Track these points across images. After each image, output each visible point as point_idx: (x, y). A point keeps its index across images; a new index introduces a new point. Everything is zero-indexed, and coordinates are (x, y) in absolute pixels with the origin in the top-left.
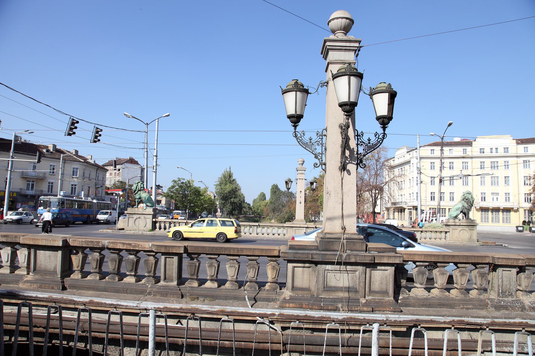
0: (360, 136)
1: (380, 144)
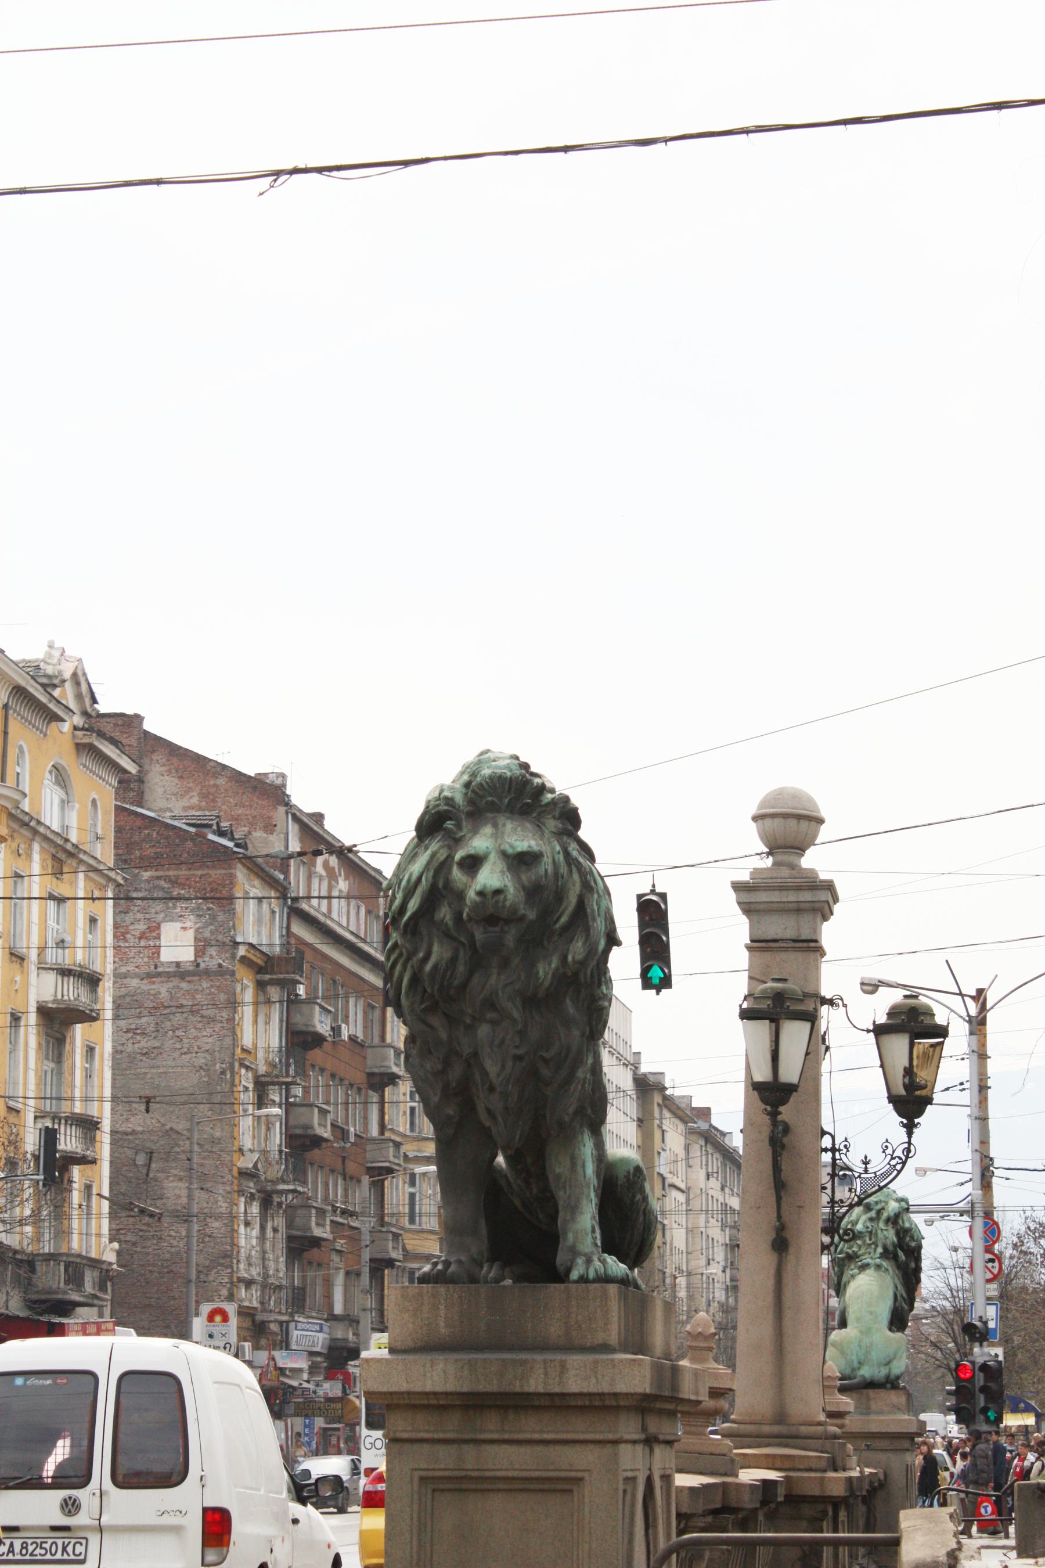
0: (839, 1150)
1: (895, 1172)
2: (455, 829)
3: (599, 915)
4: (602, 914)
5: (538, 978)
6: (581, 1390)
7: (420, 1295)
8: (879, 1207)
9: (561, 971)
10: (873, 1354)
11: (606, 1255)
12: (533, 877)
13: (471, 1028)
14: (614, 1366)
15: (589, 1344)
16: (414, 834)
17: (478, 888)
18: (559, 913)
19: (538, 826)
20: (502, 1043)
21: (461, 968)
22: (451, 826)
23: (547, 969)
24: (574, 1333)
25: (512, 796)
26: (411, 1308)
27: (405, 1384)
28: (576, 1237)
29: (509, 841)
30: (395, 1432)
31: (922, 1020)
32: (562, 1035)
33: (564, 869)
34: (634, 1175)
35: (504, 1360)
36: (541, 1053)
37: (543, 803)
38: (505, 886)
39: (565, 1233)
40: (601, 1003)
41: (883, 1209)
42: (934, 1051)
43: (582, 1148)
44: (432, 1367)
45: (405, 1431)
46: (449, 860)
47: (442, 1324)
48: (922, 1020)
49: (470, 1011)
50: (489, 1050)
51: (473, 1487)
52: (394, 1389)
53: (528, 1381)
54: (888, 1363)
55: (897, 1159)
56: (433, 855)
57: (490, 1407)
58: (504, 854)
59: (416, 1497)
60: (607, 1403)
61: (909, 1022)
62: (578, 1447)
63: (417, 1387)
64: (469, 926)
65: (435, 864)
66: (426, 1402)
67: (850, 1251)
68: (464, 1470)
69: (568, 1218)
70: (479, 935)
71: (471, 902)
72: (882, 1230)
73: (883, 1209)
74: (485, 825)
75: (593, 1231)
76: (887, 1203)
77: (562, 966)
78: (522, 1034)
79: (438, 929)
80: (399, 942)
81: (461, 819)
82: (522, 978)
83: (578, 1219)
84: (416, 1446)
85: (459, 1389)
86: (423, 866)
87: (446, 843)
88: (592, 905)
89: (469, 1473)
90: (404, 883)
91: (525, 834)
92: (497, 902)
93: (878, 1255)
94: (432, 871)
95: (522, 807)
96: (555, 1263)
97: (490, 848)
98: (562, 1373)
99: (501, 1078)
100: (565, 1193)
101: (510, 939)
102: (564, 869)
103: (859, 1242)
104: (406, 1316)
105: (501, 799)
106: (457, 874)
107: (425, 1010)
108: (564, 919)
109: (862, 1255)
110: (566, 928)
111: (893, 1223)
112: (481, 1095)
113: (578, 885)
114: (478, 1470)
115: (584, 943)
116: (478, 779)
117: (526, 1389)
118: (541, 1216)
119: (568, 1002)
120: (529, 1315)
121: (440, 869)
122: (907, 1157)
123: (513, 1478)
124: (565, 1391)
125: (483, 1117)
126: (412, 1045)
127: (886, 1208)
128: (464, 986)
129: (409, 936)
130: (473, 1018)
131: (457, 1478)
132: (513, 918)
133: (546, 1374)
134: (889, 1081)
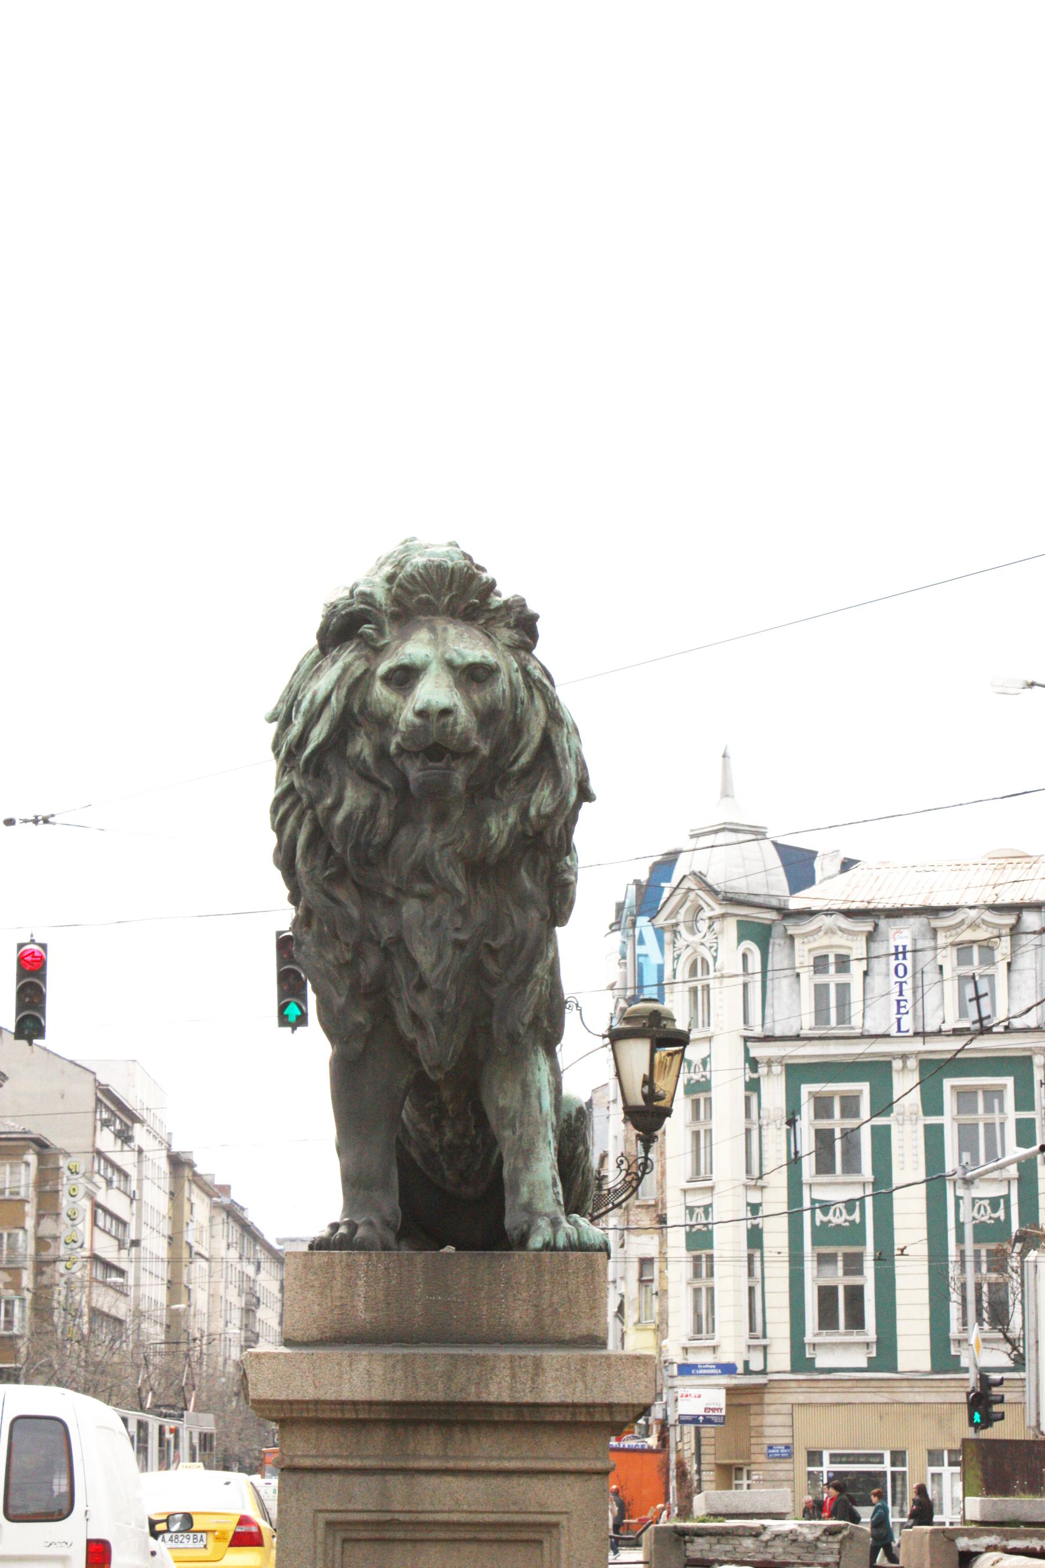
2: (375, 636)
3: (571, 756)
4: (574, 756)
5: (489, 838)
6: (563, 1399)
7: (331, 1264)
9: (520, 828)
11: (576, 1216)
12: (488, 698)
13: (392, 905)
14: (609, 1367)
15: (567, 1337)
16: (315, 642)
17: (419, 706)
18: (517, 751)
19: (489, 637)
20: (437, 924)
21: (384, 821)
22: (370, 631)
23: (501, 824)
24: (547, 1321)
25: (454, 593)
26: (317, 1284)
27: (311, 1390)
28: (532, 1191)
29: (457, 648)
30: (292, 1458)
31: (665, 1025)
32: (515, 919)
33: (523, 693)
34: (577, 1119)
35: (452, 1356)
36: (486, 941)
37: (492, 607)
38: (455, 705)
39: (516, 1189)
40: (566, 876)
42: (672, 1060)
43: (537, 1071)
44: (351, 1365)
45: (306, 1456)
46: (367, 676)
47: (361, 1306)
48: (665, 1025)
49: (393, 880)
50: (420, 934)
51: (400, 1535)
52: (297, 1396)
53: (487, 1386)
55: (633, 1175)
56: (345, 670)
57: (428, 1423)
58: (450, 665)
59: (320, 1549)
60: (597, 1418)
61: (651, 1026)
62: (551, 1480)
63: (330, 1395)
64: (398, 763)
65: (348, 680)
66: (340, 1415)
68: (389, 1511)
69: (520, 1164)
70: (414, 772)
71: (407, 726)
74: (418, 629)
75: (555, 1185)
77: (522, 823)
78: (464, 912)
79: (351, 768)
80: (297, 785)
81: (384, 622)
82: (467, 835)
83: (534, 1168)
84: (323, 1478)
85: (389, 1398)
86: (333, 683)
87: (364, 653)
88: (562, 741)
89: (396, 1516)
90: (305, 705)
91: (474, 642)
92: (444, 726)
94: (345, 689)
95: (466, 608)
96: (504, 1226)
97: (431, 656)
98: (537, 1375)
99: (436, 973)
100: (514, 1133)
101: (459, 778)
102: (523, 693)
104: (310, 1295)
105: (438, 597)
106: (380, 691)
107: (330, 879)
108: (524, 759)
110: (527, 772)
112: (405, 995)
113: (542, 714)
114: (410, 1512)
115: (553, 791)
116: (408, 568)
117: (485, 1398)
118: (447, 1173)
119: (524, 874)
120: (483, 1294)
121: (359, 685)
122: (644, 1173)
123: (459, 1524)
124: (538, 1401)
125: (404, 1024)
126: (304, 929)
128: (386, 846)
129: (311, 778)
130: (397, 890)
131: (378, 1523)
132: (464, 753)
133: (513, 1376)
134: (626, 1091)
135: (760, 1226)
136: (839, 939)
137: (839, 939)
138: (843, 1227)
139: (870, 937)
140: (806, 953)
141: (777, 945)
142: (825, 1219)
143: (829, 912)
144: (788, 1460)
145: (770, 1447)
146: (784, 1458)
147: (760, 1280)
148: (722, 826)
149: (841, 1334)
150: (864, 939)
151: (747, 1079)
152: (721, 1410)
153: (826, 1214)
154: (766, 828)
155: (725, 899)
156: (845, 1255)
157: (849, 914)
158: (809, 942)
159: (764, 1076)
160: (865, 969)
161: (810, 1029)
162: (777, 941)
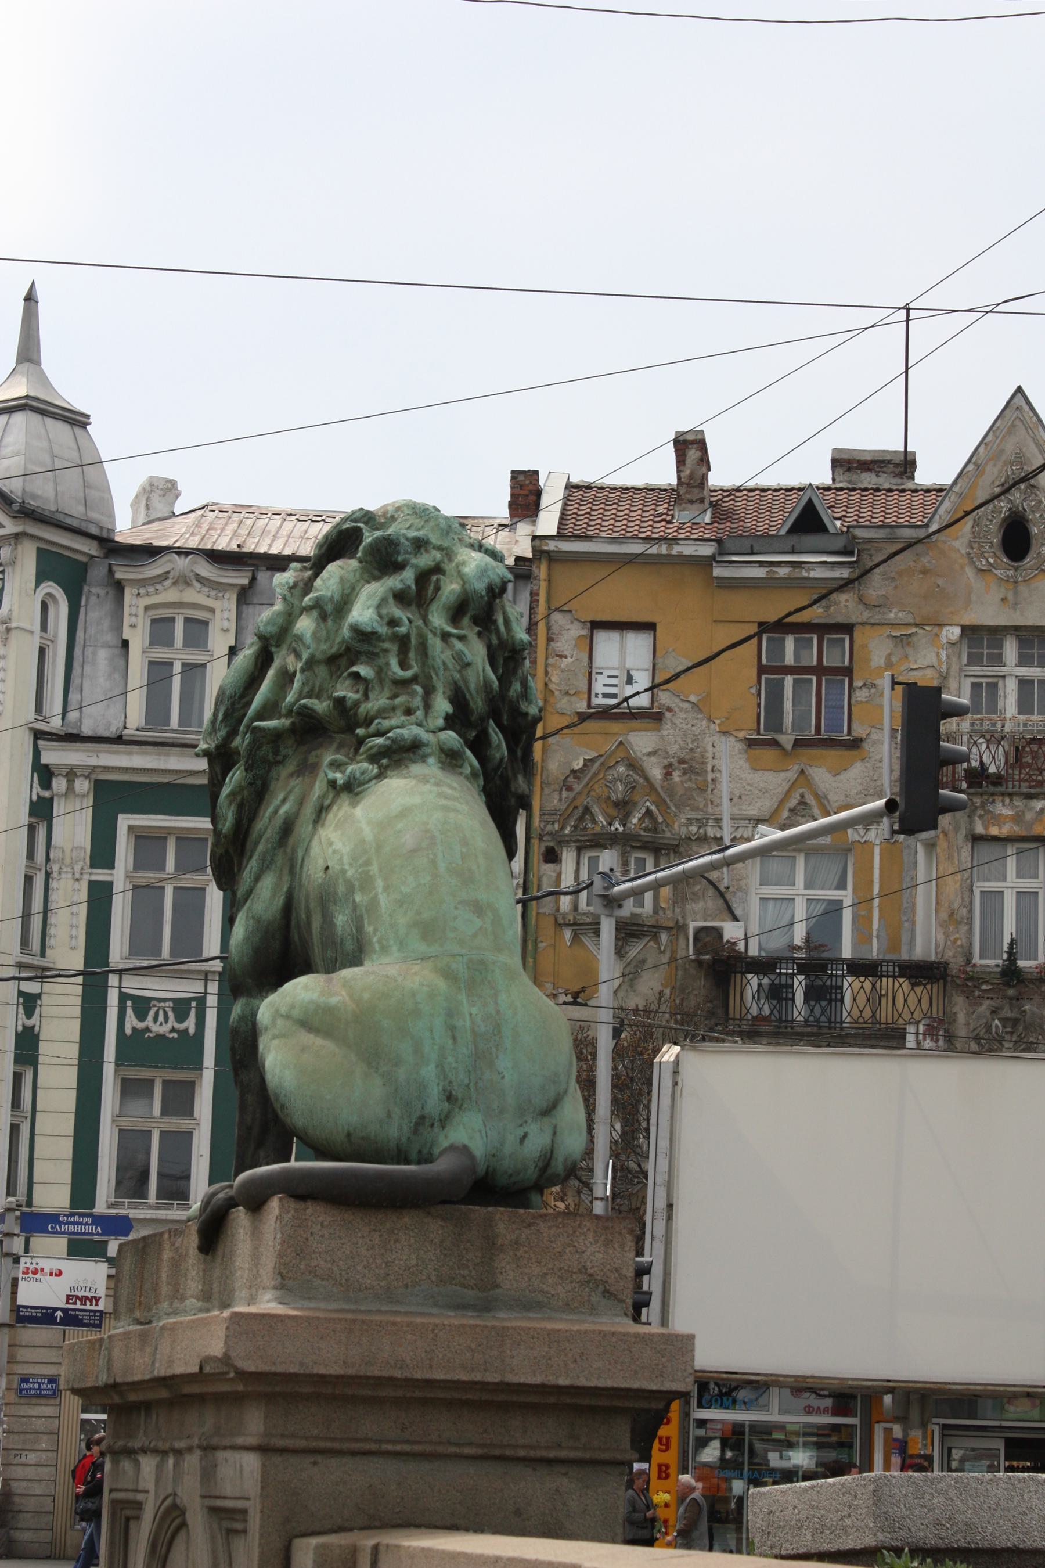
8: (425, 560)
10: (504, 1063)
41: (438, 569)
54: (549, 1110)
67: (321, 706)
72: (445, 636)
73: (438, 569)
76: (448, 553)
93: (440, 722)
103: (363, 670)
109: (382, 713)
111: (476, 621)
127: (450, 567)
135: (37, 1029)
136: (194, 595)
137: (194, 595)
138: (168, 1038)
139: (244, 596)
140: (141, 611)
141: (95, 593)
142: (140, 1025)
143: (183, 552)
144: (52, 1401)
145: (25, 1380)
146: (47, 1397)
147: (29, 1115)
148: (23, 402)
149: (150, 1207)
150: (235, 597)
151: (35, 798)
152: (98, 1300)
153: (141, 1016)
154: (88, 417)
155: (19, 512)
156: (166, 1083)
157: (217, 557)
158: (148, 595)
159: (60, 796)
160: (233, 644)
161: (138, 730)
162: (94, 590)
